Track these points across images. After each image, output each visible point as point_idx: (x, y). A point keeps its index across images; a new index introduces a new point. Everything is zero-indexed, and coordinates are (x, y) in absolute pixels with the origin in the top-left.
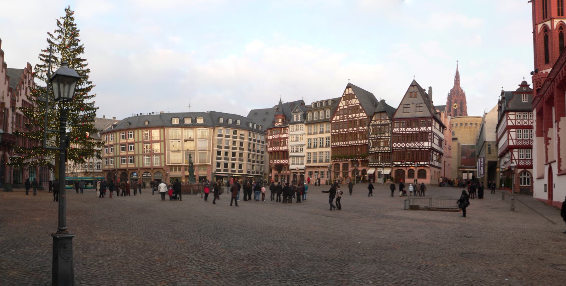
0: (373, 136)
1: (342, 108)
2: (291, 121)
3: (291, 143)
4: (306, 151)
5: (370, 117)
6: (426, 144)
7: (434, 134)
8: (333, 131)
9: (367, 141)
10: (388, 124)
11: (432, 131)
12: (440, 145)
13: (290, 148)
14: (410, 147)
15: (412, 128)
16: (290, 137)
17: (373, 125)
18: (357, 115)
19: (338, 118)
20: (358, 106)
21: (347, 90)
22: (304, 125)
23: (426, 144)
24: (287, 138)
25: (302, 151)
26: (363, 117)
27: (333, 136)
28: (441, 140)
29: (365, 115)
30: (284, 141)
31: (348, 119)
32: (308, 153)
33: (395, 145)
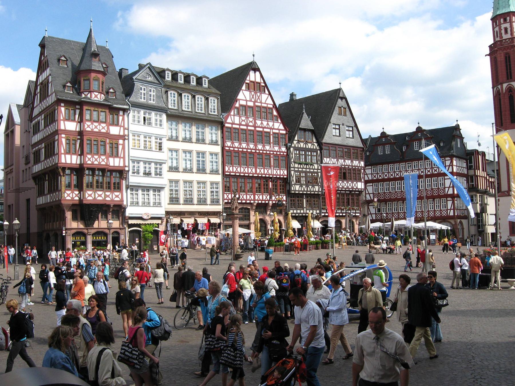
0: (296, 166)
1: (243, 103)
2: (133, 98)
3: (135, 153)
4: (168, 175)
8: (229, 144)
10: (315, 151)
13: (130, 162)
14: (343, 187)
16: (131, 135)
18: (271, 124)
19: (237, 120)
20: (272, 109)
21: (252, 73)
22: (164, 116)
24: (123, 137)
25: (159, 174)
29: (282, 127)
30: (113, 145)
31: (255, 127)
32: (171, 181)
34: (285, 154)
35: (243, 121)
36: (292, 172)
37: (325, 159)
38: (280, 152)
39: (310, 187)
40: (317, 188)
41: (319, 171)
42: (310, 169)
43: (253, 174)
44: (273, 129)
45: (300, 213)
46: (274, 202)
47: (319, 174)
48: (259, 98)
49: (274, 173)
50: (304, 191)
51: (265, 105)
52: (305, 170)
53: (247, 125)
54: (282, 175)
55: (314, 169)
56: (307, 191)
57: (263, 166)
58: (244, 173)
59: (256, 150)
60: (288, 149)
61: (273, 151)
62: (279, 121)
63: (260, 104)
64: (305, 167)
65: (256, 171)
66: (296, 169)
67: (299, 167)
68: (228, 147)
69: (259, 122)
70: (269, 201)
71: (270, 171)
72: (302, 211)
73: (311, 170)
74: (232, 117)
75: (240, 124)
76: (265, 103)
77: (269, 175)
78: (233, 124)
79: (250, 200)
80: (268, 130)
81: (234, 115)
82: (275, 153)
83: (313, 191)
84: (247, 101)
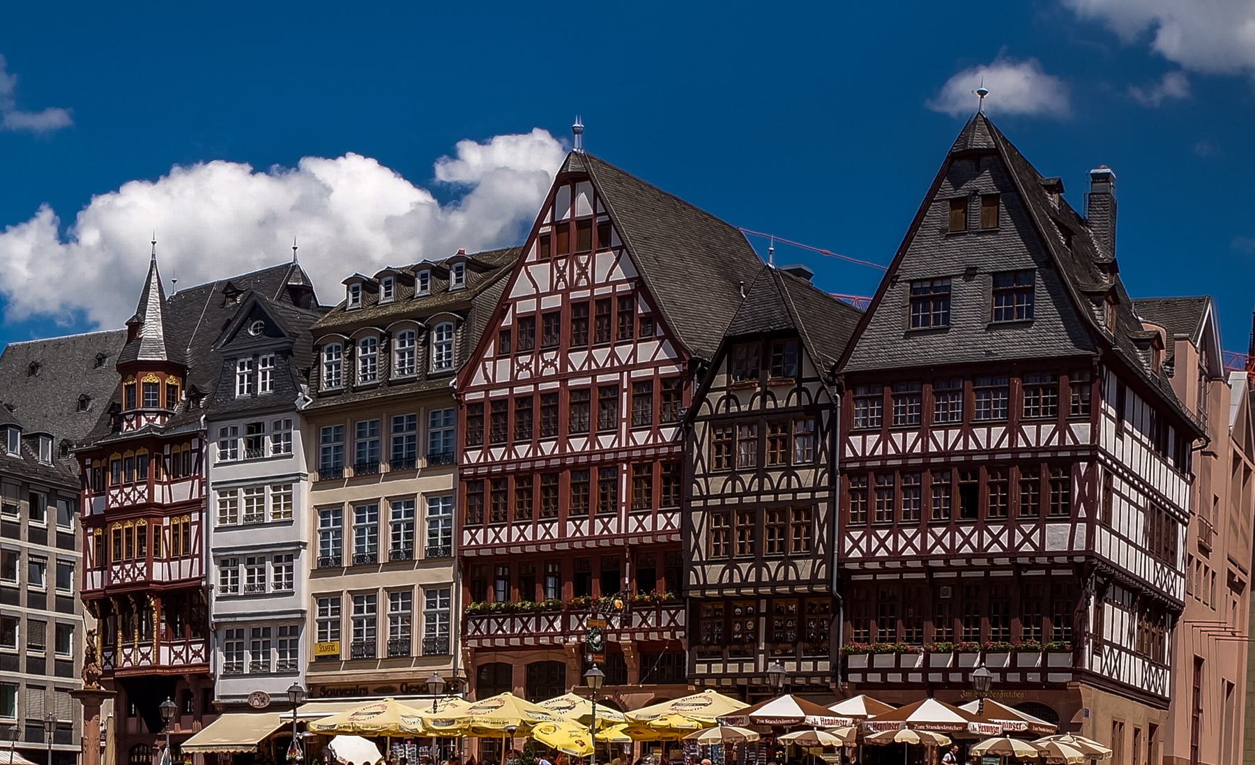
0: (717, 485)
5: (698, 370)
6: (1057, 536)
7: (1116, 468)
8: (474, 456)
9: (676, 520)
11: (1094, 447)
12: (1160, 545)
15: (967, 432)
17: (715, 421)
18: (624, 352)
19: (503, 369)
23: (1057, 536)
26: (655, 364)
27: (472, 483)
28: (1162, 519)
33: (855, 545)
34: (678, 449)
35: (521, 367)
36: (696, 517)
37: (856, 440)
38: (656, 446)
39: (773, 565)
40: (805, 568)
41: (818, 495)
42: (776, 491)
43: (553, 542)
44: (629, 368)
45: (741, 675)
46: (640, 637)
47: (823, 509)
48: (583, 271)
49: (631, 530)
50: (745, 583)
51: (609, 290)
52: (754, 499)
53: (536, 379)
54: (664, 532)
55: (795, 492)
56: (759, 583)
57: (581, 510)
58: (523, 545)
59: (563, 456)
60: (686, 426)
61: (628, 449)
62: (660, 332)
63: (587, 293)
64: (755, 488)
65: (563, 530)
66: (710, 502)
67: (728, 490)
68: (470, 466)
69: (577, 359)
70: (619, 633)
71: (613, 525)
72: (749, 668)
73: (781, 497)
74: (489, 365)
75: (514, 382)
76: (607, 284)
77: (611, 537)
78: (493, 386)
79: (552, 636)
80: (615, 377)
81: (494, 359)
82: (637, 454)
83: (786, 582)
84: (538, 296)
